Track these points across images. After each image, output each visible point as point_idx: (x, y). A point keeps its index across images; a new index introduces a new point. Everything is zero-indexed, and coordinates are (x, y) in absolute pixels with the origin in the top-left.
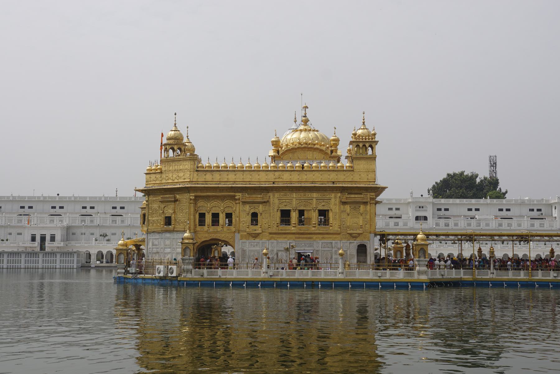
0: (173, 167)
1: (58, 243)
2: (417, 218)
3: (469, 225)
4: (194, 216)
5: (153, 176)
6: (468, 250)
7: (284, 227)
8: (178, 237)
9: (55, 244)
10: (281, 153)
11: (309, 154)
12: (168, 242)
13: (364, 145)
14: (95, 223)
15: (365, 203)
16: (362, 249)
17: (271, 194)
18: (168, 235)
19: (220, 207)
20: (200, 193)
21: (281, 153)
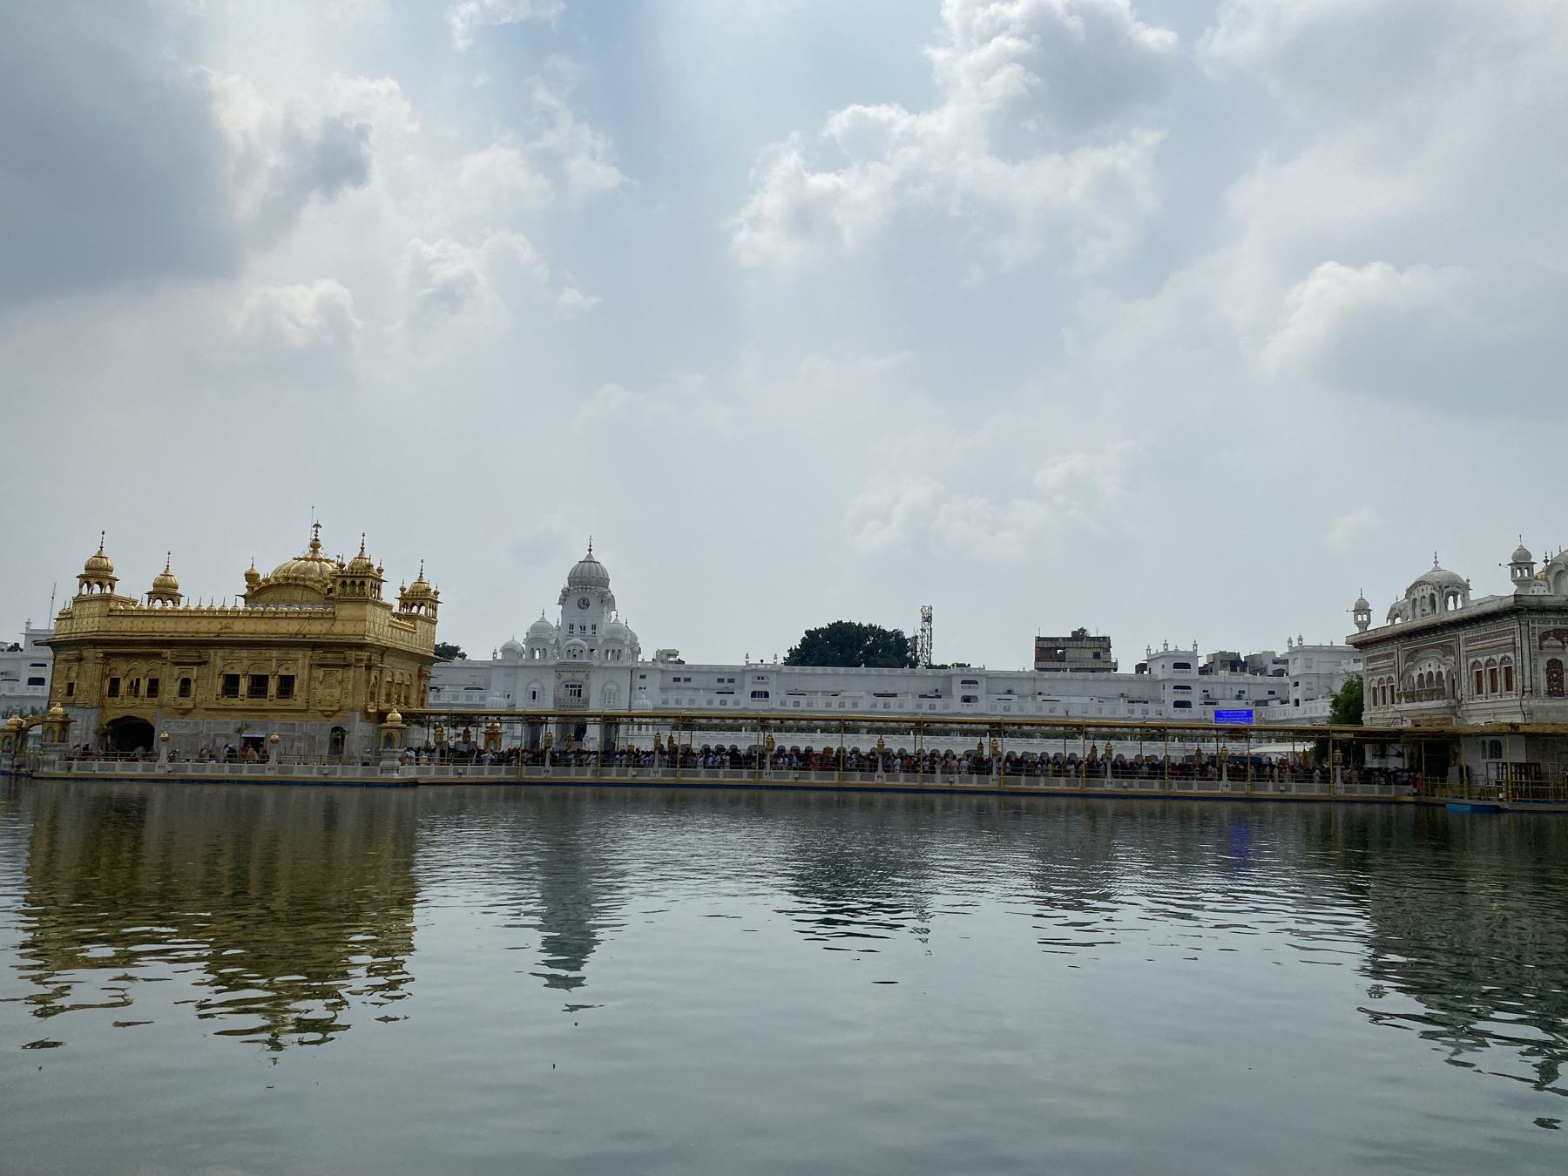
3: (828, 705)
7: (228, 702)
10: (257, 589)
11: (297, 594)
13: (353, 583)
15: (346, 666)
17: (212, 652)
19: (142, 670)
20: (115, 648)
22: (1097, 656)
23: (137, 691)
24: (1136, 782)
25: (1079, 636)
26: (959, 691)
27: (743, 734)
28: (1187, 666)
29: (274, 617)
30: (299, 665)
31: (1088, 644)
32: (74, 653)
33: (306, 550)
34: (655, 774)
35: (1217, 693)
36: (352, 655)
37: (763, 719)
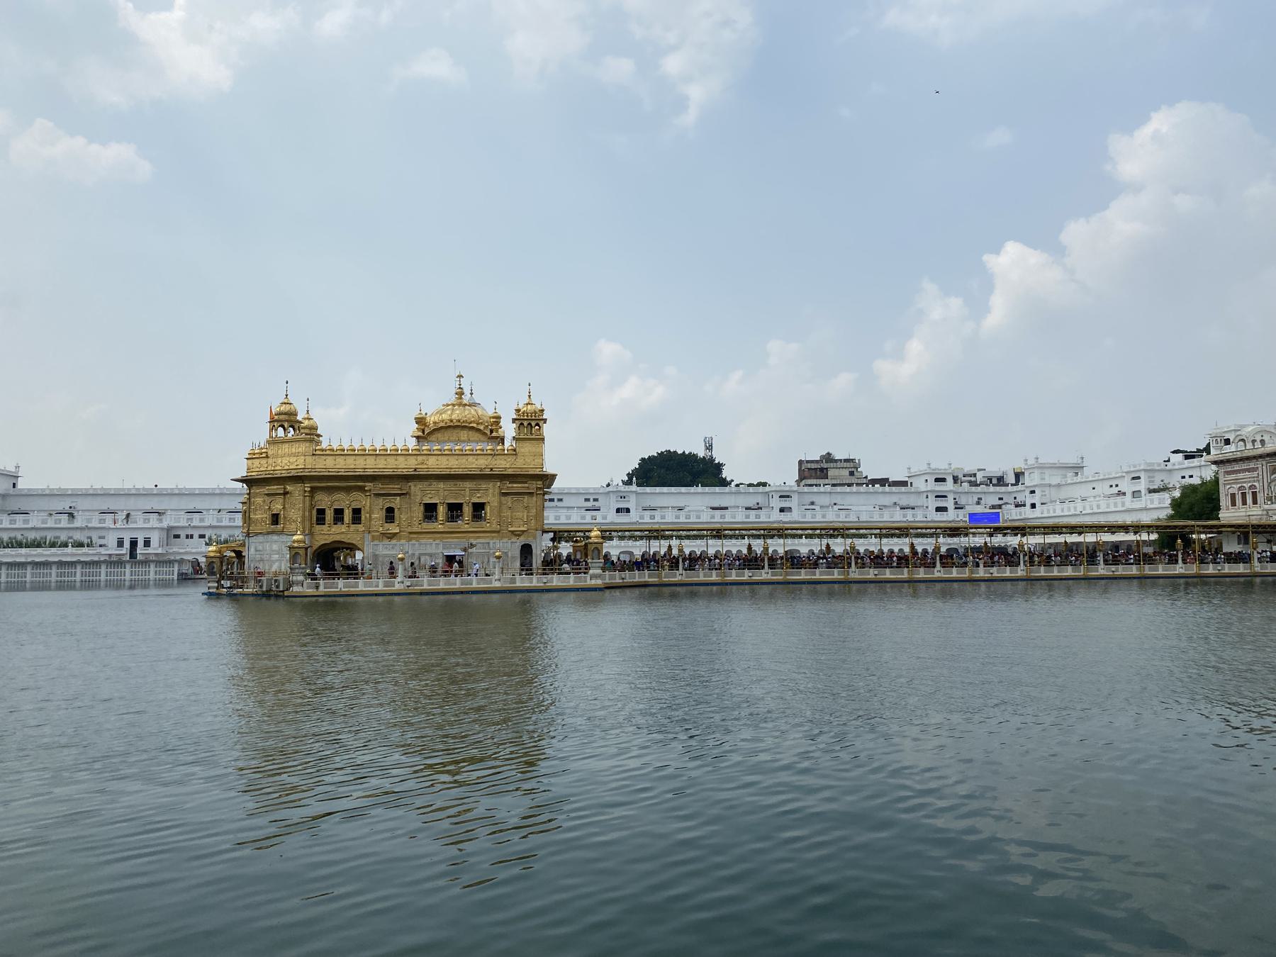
0: (286, 448)
1: (155, 548)
2: (618, 510)
3: (678, 517)
4: (310, 512)
5: (257, 462)
6: (638, 549)
8: (288, 540)
9: (150, 550)
10: (426, 431)
11: (464, 434)
12: (275, 547)
14: (206, 524)
16: (526, 550)
18: (275, 537)
19: (346, 502)
21: (426, 431)
22: (852, 474)
23: (342, 520)
24: (1120, 567)
25: (828, 458)
26: (777, 503)
27: (615, 542)
28: (943, 480)
29: (462, 454)
30: (489, 494)
31: (845, 465)
32: (274, 488)
33: (452, 398)
34: (765, 574)
35: (962, 501)
36: (533, 485)
37: (718, 530)
